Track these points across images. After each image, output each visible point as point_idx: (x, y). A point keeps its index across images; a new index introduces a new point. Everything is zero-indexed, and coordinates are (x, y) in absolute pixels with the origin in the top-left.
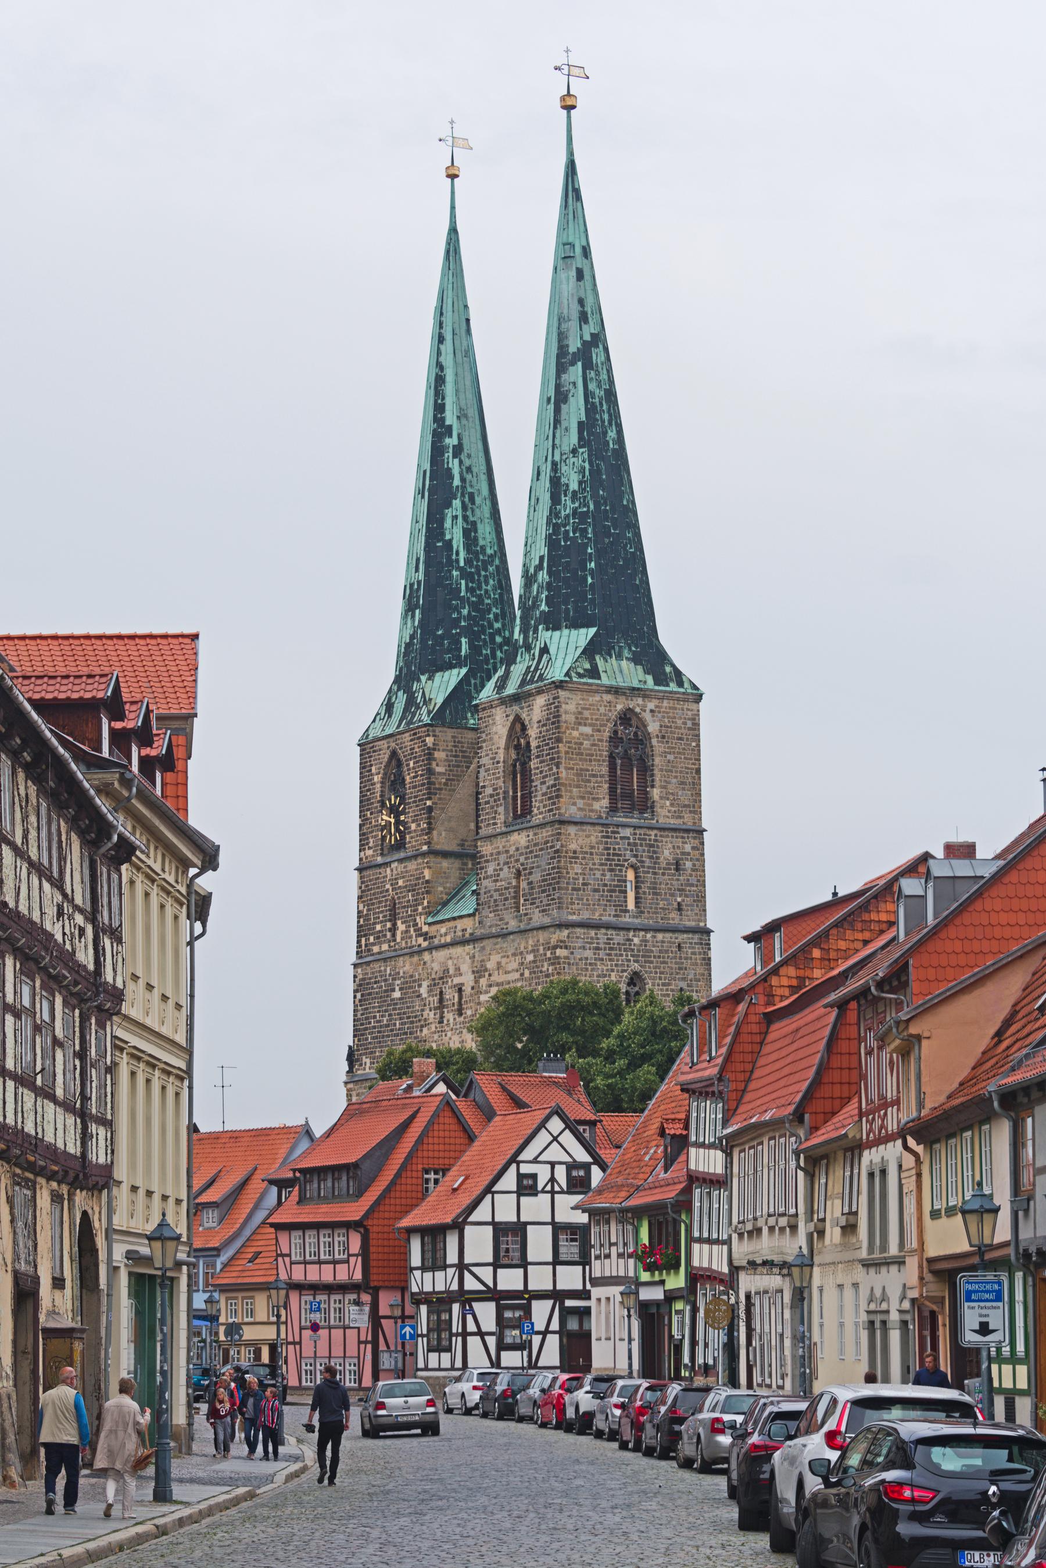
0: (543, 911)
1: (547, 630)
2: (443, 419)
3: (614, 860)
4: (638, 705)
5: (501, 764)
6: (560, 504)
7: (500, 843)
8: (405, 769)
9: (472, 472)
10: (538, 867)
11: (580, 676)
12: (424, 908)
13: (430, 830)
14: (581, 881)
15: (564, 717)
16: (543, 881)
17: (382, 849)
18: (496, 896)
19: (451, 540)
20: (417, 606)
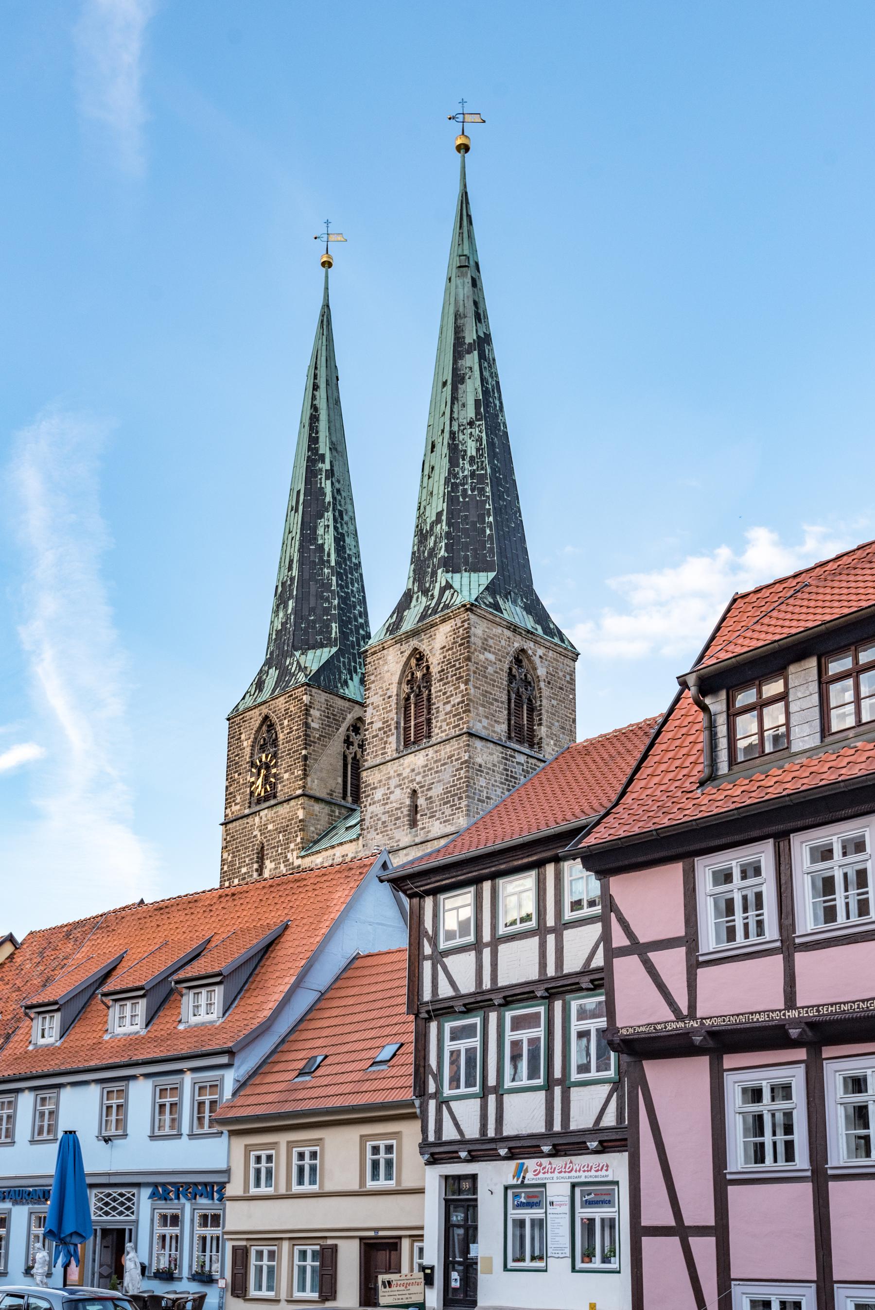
0: (445, 822)
1: (447, 572)
2: (317, 449)
3: (511, 781)
5: (394, 698)
6: (458, 467)
7: (391, 768)
8: (278, 728)
9: (341, 494)
10: (439, 782)
11: (487, 605)
12: (296, 845)
13: (305, 775)
14: (485, 795)
15: (472, 639)
17: (250, 803)
19: (323, 545)
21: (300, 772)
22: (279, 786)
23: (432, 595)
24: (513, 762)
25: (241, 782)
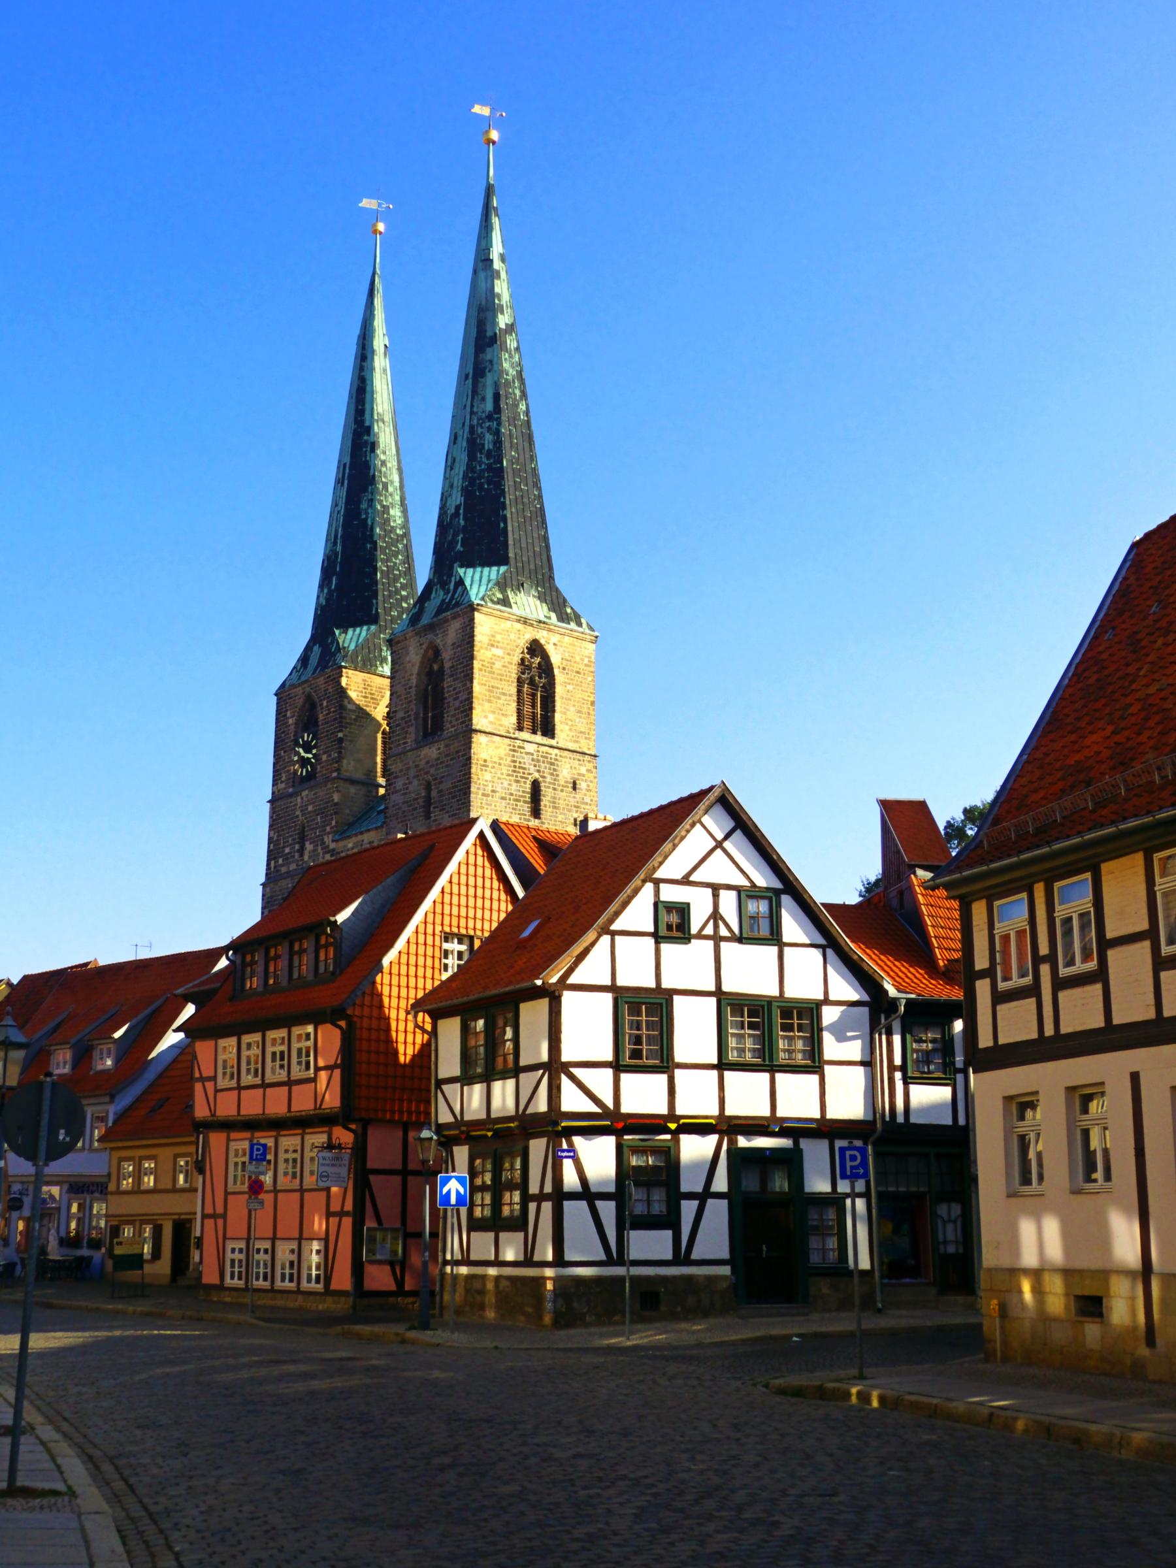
0: (453, 815)
2: (363, 421)
3: (519, 772)
4: (543, 637)
5: (414, 689)
9: (386, 466)
12: (331, 828)
13: (339, 760)
16: (453, 788)
17: (293, 782)
18: (404, 807)
19: (366, 519)
20: (334, 573)
21: (336, 755)
22: (319, 767)
23: (449, 589)
24: (521, 753)
25: (287, 760)
